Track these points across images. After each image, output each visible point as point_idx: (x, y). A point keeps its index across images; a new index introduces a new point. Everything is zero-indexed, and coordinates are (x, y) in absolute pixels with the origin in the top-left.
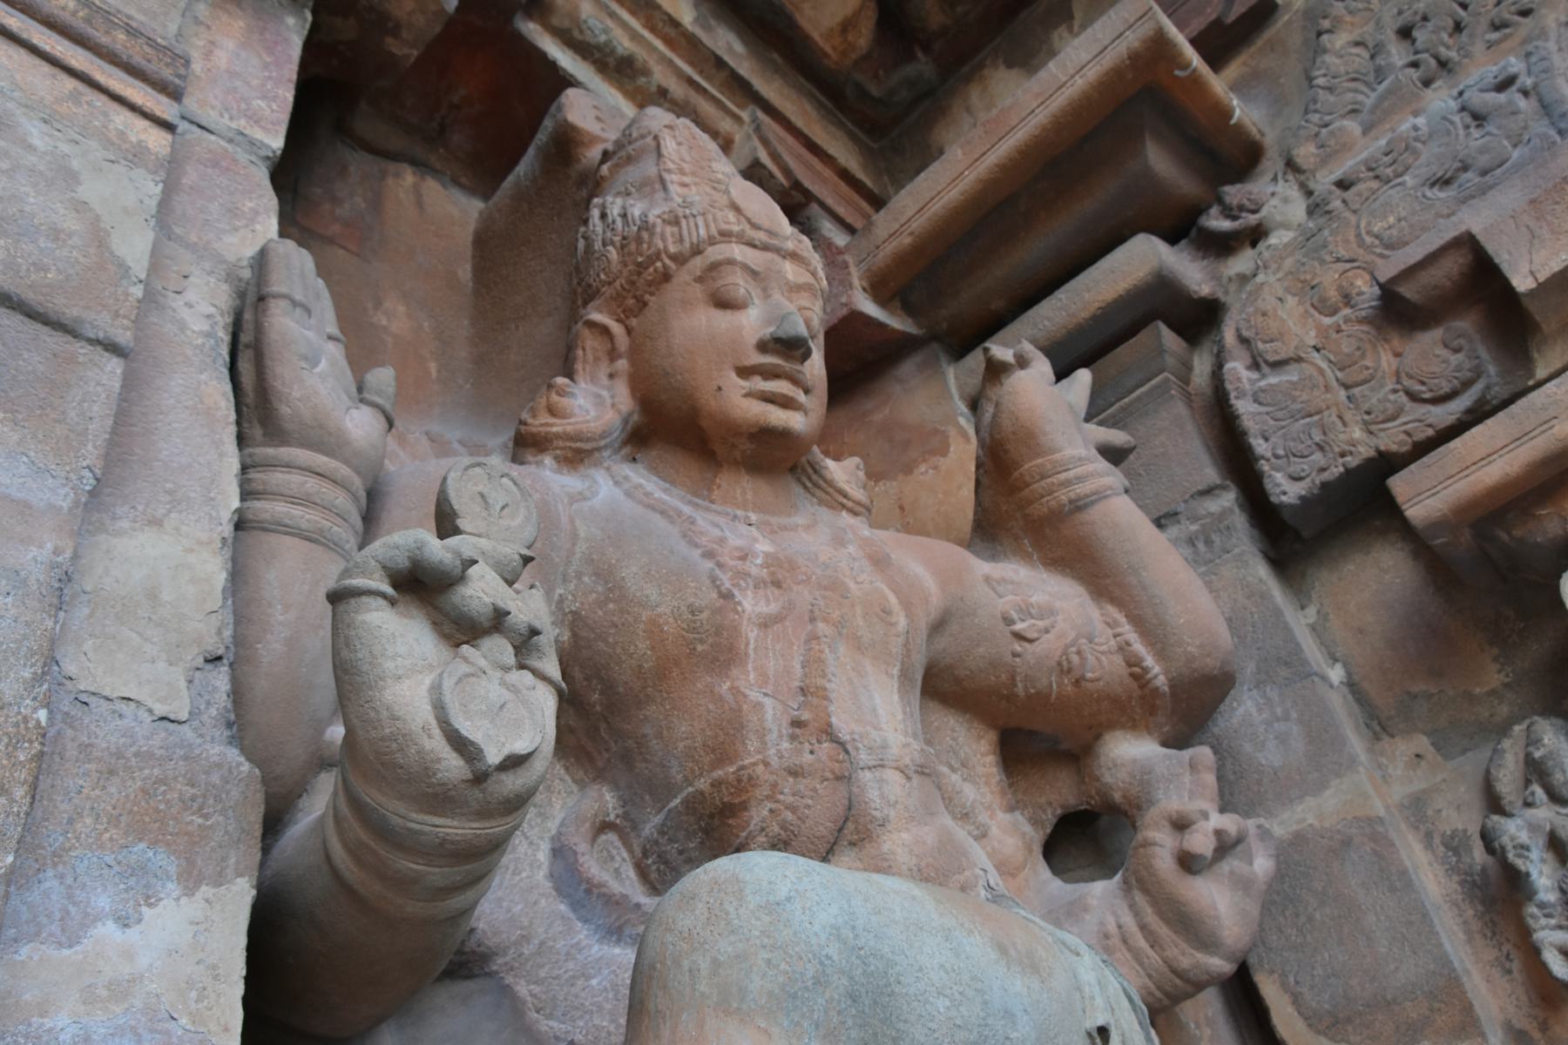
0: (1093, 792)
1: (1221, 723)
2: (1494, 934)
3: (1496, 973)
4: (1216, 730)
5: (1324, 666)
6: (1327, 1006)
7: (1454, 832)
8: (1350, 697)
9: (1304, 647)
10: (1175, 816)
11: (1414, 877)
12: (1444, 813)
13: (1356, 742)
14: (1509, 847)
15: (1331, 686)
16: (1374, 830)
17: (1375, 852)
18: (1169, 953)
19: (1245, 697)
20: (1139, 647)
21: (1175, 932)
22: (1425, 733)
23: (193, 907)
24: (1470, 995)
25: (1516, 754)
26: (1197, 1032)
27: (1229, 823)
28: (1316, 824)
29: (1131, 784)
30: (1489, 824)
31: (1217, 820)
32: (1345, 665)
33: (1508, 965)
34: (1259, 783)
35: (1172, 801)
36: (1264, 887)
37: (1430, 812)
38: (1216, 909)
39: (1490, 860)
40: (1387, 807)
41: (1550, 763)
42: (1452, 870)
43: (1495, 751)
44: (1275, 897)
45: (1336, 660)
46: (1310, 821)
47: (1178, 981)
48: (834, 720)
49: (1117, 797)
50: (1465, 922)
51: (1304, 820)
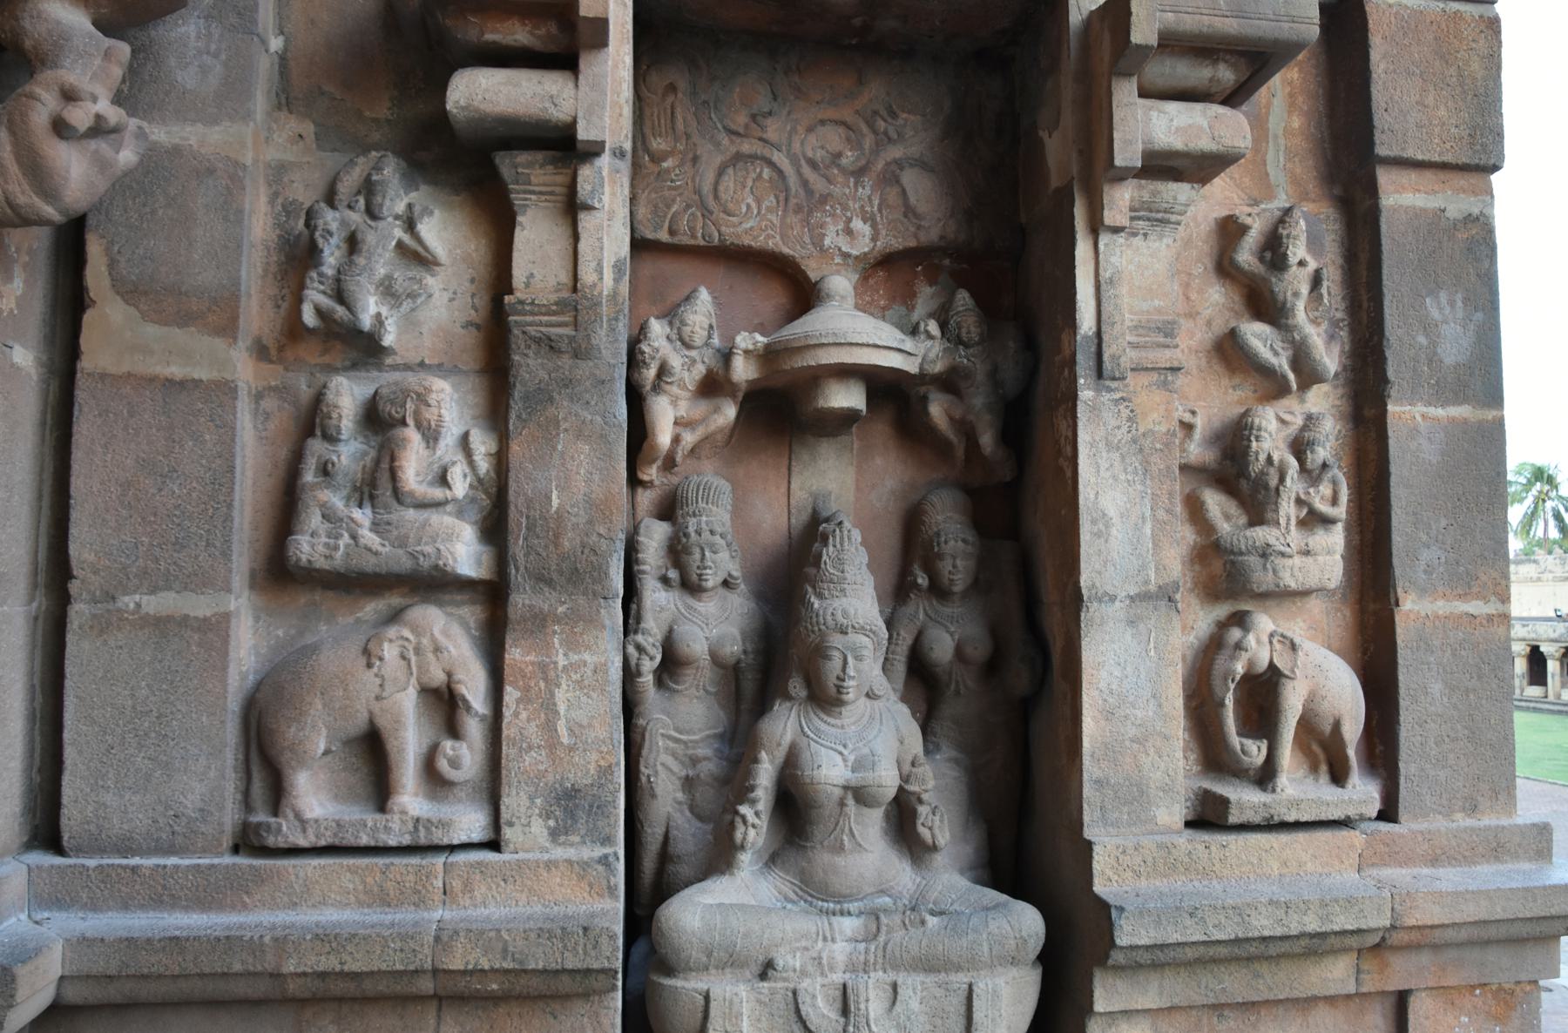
0: (7, 28)
1: (161, 29)
2: (283, 279)
3: (269, 305)
4: (153, 33)
5: (271, 31)
6: (134, 278)
7: (294, 200)
8: (277, 67)
9: (261, 10)
10: (67, 87)
11: (246, 217)
12: (295, 185)
13: (260, 102)
14: (320, 228)
15: (267, 51)
16: (235, 175)
17: (228, 188)
18: (10, 188)
19: (192, 21)
21: (24, 174)
22: (314, 122)
24: (241, 310)
25: (363, 170)
26: (15, 255)
27: (113, 114)
28: (195, 147)
29: (46, 40)
30: (316, 207)
31: (104, 106)
32: (287, 41)
33: (280, 302)
34: (167, 94)
35: (73, 74)
36: (120, 173)
37: (285, 179)
38: (68, 172)
39: (306, 232)
40: (256, 161)
41: (379, 188)
42: (278, 225)
43: (351, 160)
44: (134, 185)
45: (282, 33)
46: (191, 142)
47: (9, 211)
49: (28, 44)
50: (267, 263)
51: (188, 139)
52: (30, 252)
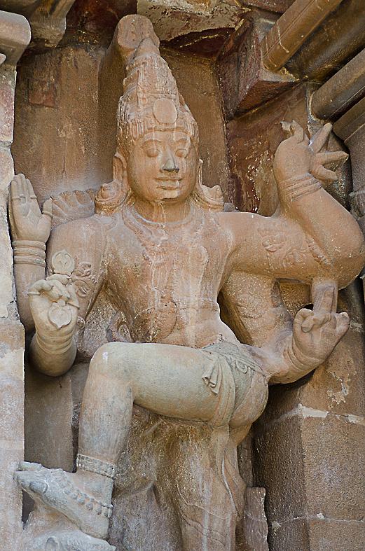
20: (318, 250)
23: (13, 354)
48: (173, 296)
52: (351, 377)
